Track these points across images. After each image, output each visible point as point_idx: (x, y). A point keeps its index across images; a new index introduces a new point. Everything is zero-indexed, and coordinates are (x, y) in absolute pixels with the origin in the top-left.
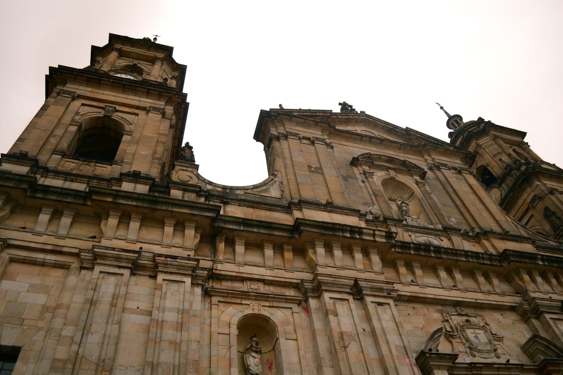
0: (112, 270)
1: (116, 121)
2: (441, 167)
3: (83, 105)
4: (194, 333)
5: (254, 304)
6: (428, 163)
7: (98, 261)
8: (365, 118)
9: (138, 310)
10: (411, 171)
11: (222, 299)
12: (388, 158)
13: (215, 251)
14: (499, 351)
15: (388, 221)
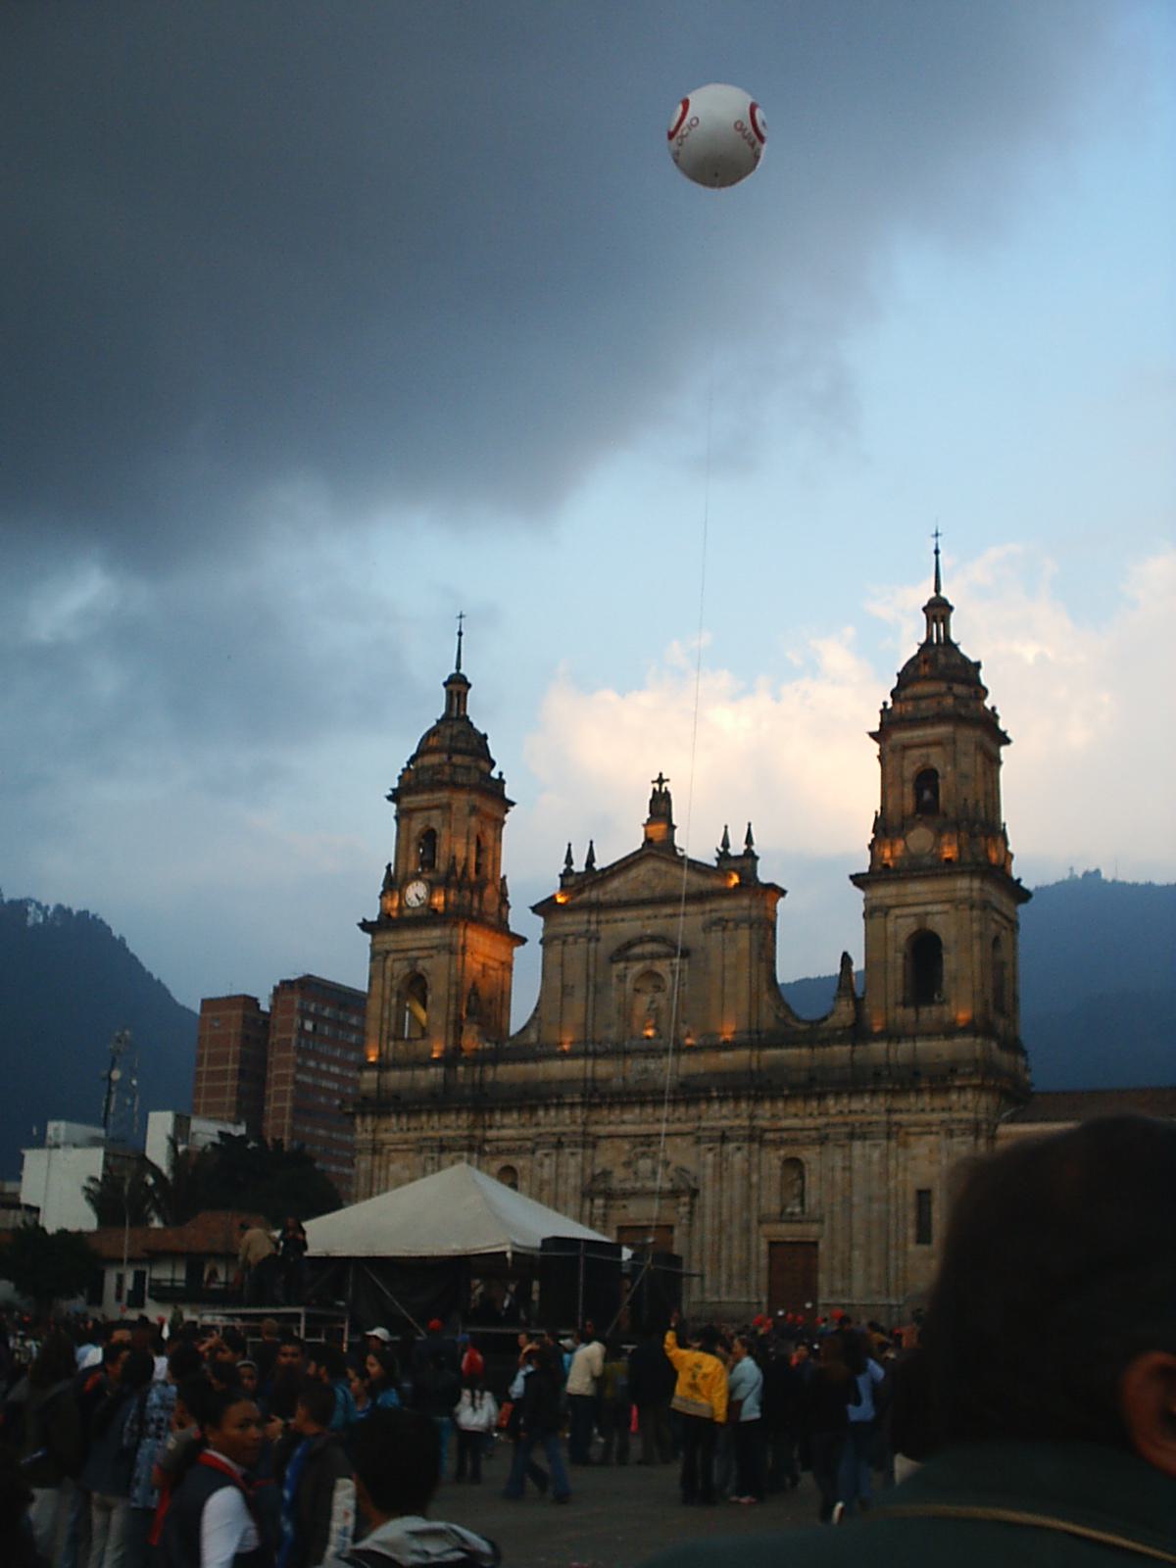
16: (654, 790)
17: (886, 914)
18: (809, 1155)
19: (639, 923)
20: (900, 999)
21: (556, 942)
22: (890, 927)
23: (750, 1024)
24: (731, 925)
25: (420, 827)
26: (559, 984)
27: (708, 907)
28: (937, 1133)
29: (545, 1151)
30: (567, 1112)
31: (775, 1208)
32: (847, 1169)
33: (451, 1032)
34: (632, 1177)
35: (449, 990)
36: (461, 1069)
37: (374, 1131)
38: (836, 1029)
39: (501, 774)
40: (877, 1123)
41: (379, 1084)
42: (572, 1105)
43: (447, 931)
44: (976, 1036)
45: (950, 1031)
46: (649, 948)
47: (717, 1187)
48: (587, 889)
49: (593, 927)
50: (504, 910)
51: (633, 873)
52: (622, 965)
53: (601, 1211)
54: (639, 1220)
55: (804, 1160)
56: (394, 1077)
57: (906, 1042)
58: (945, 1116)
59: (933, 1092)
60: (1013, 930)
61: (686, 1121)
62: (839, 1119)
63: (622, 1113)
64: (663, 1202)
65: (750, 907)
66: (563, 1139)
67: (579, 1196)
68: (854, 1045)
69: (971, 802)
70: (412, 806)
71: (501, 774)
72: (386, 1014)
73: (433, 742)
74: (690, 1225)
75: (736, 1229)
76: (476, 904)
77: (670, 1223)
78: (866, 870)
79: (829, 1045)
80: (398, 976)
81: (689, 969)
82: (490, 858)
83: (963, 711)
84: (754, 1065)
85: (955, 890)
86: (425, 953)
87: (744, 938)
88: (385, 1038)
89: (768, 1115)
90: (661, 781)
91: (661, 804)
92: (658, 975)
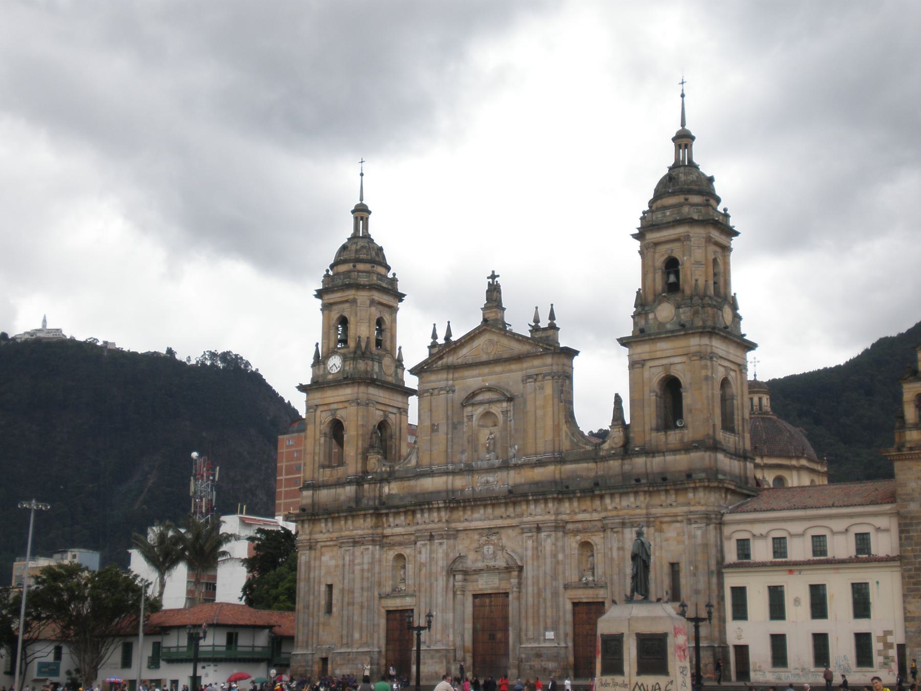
0: (348, 548)
3: (321, 411)
4: (377, 569)
7: (343, 545)
13: (383, 523)
14: (498, 557)
16: (489, 282)
17: (643, 365)
18: (596, 539)
19: (480, 378)
20: (654, 425)
21: (426, 394)
22: (647, 374)
23: (554, 446)
24: (540, 377)
25: (338, 316)
26: (429, 424)
27: (525, 365)
28: (681, 522)
29: (423, 542)
30: (435, 514)
31: (575, 578)
32: (619, 549)
33: (360, 461)
34: (479, 558)
35: (357, 431)
36: (366, 486)
37: (311, 533)
38: (613, 448)
39: (394, 274)
40: (640, 515)
41: (313, 500)
42: (439, 509)
43: (356, 389)
44: (705, 451)
45: (687, 448)
46: (487, 396)
47: (535, 564)
48: (444, 356)
49: (450, 382)
50: (399, 371)
51: (476, 343)
52: (469, 409)
53: (460, 583)
54: (486, 589)
55: (593, 543)
56: (325, 495)
57: (659, 456)
58: (685, 509)
59: (677, 491)
60: (741, 371)
61: (514, 518)
62: (615, 513)
63: (472, 513)
64: (502, 575)
65: (552, 365)
66: (433, 534)
67: (444, 573)
68: (623, 459)
69: (701, 282)
70: (332, 301)
71: (394, 274)
72: (317, 450)
73: (345, 256)
74: (519, 592)
75: (548, 595)
76: (376, 368)
77: (507, 591)
78: (631, 335)
79: (607, 461)
80: (325, 422)
81: (514, 410)
82: (389, 334)
83: (696, 217)
84: (557, 476)
85: (689, 346)
86: (340, 406)
87: (549, 387)
88: (317, 465)
89: (568, 511)
90: (493, 276)
91: (494, 292)
92: (493, 414)
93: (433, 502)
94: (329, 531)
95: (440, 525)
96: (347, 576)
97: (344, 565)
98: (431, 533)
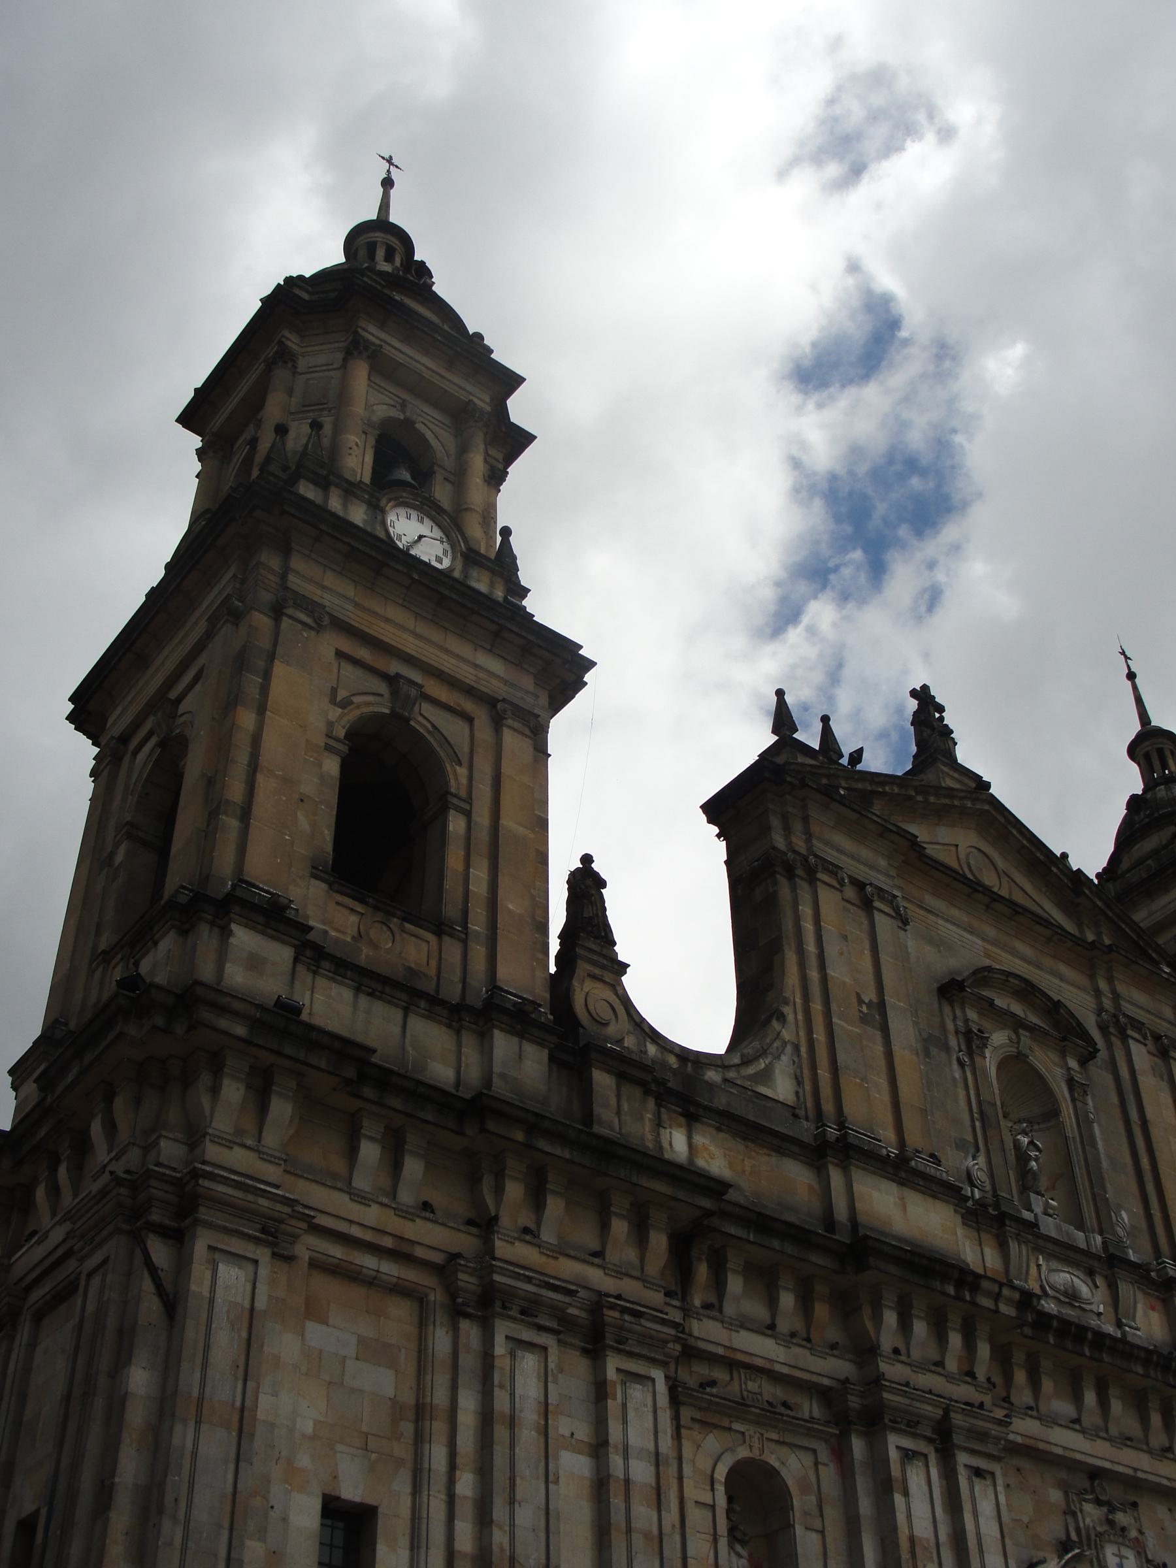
0: (527, 1335)
1: (422, 737)
2: (1130, 1032)
3: (339, 654)
5: (752, 1432)
6: (1100, 1010)
8: (986, 807)
9: (573, 1441)
10: (1066, 1043)
11: (698, 1415)
12: (1023, 985)
15: (1007, 1222)
36: (602, 1080)
66: (957, 1419)
72: (309, 785)
93: (985, 1284)
94: (393, 1194)
95: (963, 1391)
96: (529, 1488)
97: (512, 1422)
98: (947, 1411)
